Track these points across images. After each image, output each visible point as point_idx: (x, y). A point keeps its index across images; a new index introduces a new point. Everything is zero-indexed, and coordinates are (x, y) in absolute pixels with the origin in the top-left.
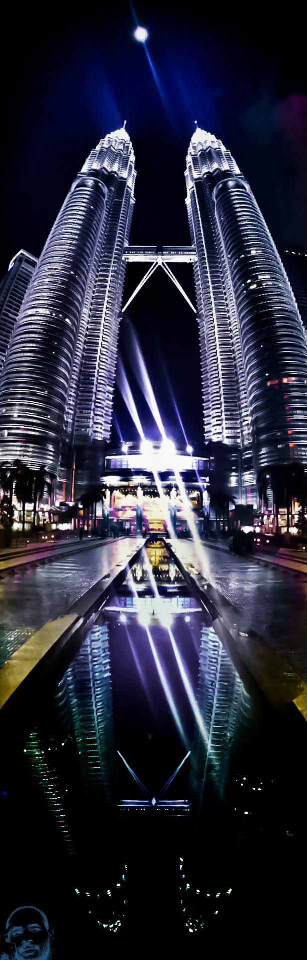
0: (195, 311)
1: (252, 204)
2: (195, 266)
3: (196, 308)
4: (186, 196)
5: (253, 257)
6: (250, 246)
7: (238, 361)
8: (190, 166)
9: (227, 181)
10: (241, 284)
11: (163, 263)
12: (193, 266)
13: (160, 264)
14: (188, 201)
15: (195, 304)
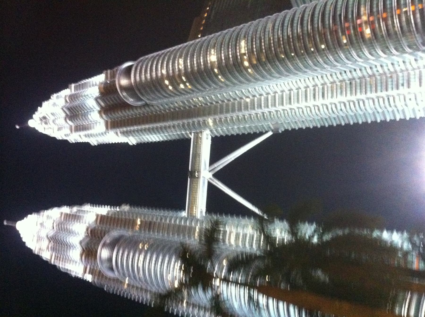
0: (270, 134)
1: (154, 58)
2: (217, 134)
3: (266, 132)
4: (127, 143)
5: (219, 60)
6: (205, 62)
7: (335, 79)
8: (86, 136)
9: (121, 87)
10: (249, 74)
11: (210, 171)
12: (216, 137)
13: (210, 175)
14: (132, 141)
15: (261, 134)
